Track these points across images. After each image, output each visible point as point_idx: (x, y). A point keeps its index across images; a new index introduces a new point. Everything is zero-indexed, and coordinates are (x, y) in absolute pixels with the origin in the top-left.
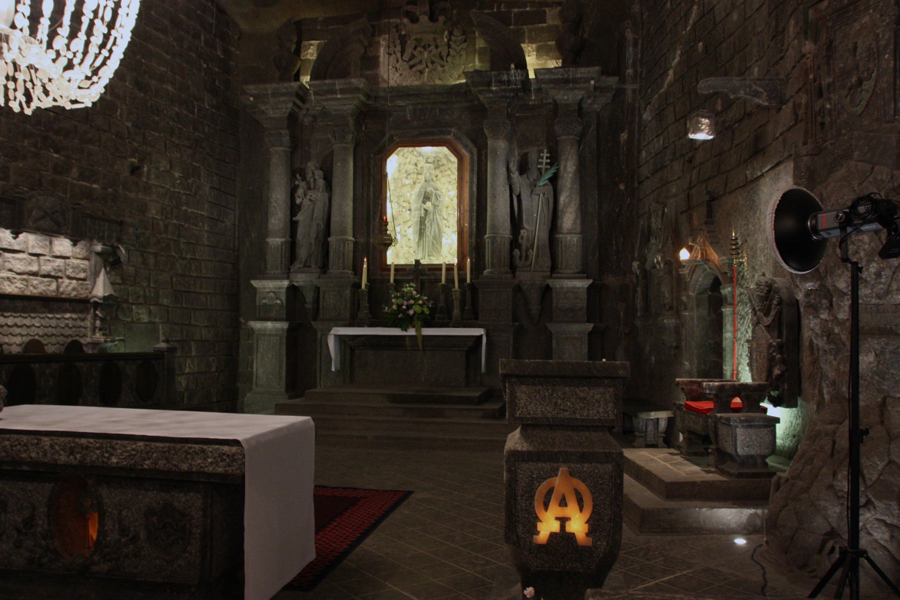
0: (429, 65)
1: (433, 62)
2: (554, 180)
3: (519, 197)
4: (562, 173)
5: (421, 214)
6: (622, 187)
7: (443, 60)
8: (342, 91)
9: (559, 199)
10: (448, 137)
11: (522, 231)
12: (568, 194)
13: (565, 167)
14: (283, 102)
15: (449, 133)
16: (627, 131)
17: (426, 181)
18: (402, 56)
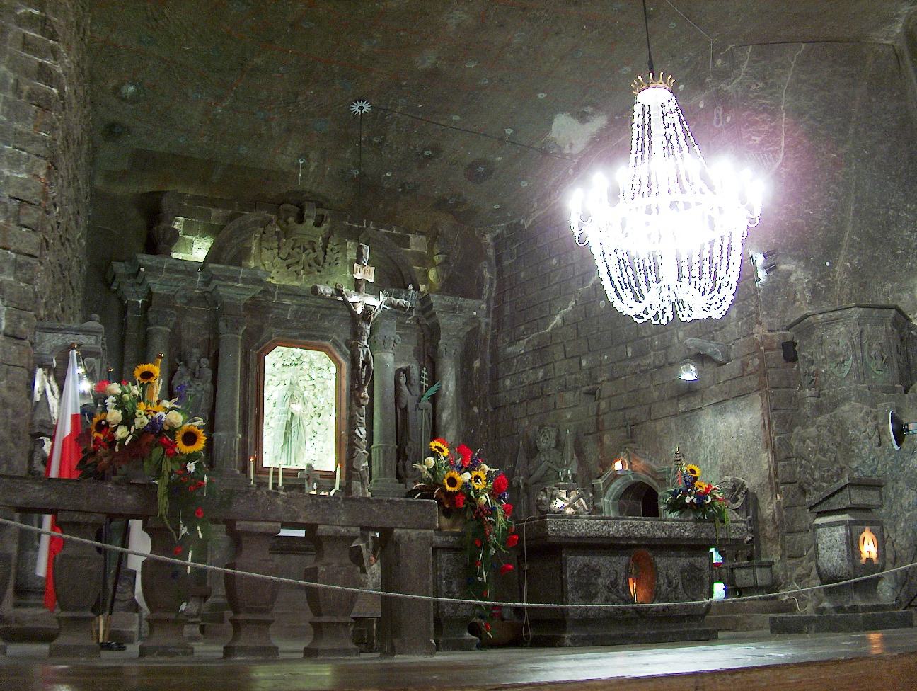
0: (307, 268)
1: (310, 266)
2: (434, 399)
3: (405, 410)
4: (444, 392)
5: (287, 417)
6: (476, 410)
7: (319, 265)
8: (245, 281)
9: (440, 417)
10: (327, 343)
11: (409, 443)
12: (450, 412)
13: (447, 387)
14: (176, 279)
15: (328, 339)
16: (479, 360)
17: (291, 383)
18: (278, 254)
